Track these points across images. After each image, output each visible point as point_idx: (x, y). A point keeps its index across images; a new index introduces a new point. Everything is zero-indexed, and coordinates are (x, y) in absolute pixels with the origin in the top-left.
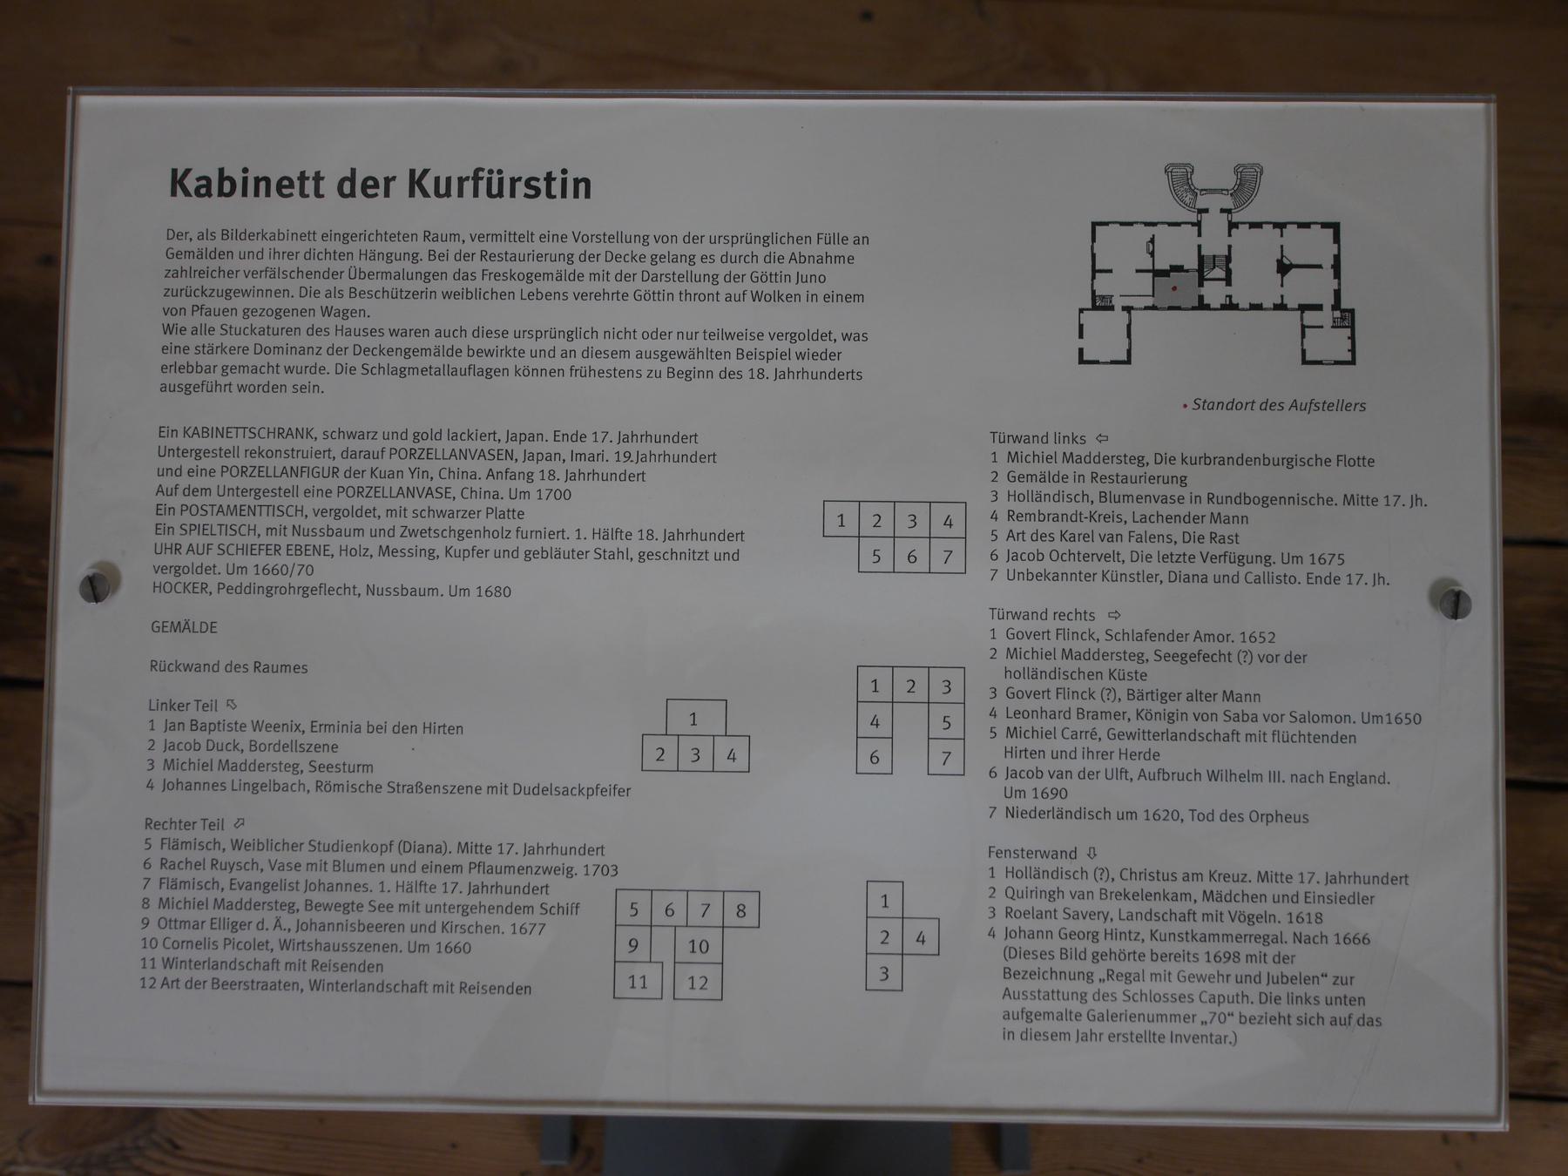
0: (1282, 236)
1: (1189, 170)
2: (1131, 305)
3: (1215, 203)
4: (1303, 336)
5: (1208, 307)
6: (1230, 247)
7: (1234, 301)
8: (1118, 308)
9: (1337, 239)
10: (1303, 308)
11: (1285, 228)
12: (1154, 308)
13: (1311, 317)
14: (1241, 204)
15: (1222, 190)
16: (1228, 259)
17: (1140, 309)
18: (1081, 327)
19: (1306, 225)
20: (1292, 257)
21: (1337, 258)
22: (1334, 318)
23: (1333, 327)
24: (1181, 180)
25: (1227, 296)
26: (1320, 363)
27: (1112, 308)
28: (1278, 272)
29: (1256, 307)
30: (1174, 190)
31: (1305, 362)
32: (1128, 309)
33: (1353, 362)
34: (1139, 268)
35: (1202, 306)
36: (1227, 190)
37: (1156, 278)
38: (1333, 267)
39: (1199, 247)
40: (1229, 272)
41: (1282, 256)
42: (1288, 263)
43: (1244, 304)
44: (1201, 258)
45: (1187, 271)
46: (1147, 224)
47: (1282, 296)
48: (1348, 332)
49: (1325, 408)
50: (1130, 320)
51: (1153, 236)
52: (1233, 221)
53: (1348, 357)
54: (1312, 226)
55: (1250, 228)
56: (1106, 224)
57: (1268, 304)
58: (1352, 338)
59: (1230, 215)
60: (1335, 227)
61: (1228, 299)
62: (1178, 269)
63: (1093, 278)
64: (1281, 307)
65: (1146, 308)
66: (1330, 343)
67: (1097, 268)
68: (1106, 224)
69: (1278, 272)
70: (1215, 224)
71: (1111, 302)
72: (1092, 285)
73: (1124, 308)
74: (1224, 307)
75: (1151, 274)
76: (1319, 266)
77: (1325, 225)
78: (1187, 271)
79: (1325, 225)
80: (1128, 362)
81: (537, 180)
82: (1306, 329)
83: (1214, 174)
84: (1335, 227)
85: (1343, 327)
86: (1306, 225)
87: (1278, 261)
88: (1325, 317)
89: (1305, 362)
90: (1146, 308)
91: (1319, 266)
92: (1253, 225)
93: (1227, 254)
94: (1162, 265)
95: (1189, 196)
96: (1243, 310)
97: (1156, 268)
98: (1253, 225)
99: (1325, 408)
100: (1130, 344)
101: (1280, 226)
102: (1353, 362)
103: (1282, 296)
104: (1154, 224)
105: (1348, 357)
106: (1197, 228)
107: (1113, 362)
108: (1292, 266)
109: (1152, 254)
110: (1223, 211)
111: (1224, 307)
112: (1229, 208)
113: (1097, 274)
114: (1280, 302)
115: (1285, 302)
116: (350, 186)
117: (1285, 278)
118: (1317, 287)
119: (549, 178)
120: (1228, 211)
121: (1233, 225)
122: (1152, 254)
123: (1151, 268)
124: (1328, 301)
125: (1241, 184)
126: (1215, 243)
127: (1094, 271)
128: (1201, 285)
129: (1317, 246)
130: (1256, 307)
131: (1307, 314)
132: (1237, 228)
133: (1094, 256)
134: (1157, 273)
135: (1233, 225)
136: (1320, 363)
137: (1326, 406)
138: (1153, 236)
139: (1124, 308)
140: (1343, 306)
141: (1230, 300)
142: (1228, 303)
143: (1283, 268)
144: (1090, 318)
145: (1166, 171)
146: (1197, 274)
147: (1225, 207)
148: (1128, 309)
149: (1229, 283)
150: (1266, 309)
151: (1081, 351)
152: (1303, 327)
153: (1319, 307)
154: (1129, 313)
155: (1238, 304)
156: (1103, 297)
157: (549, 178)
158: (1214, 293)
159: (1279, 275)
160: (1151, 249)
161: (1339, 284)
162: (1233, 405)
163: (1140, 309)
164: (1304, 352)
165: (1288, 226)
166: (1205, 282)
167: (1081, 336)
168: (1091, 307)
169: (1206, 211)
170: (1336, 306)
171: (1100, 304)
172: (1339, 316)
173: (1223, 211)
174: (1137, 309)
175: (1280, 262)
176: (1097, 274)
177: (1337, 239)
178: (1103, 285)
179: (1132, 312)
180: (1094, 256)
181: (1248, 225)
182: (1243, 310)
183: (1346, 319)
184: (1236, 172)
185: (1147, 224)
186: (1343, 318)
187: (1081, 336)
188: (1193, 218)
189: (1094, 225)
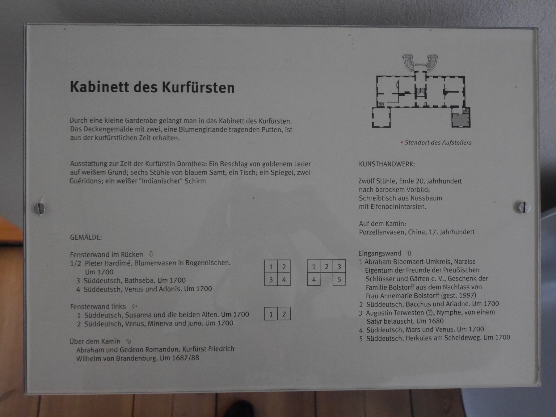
0: (445, 81)
3: (421, 69)
5: (418, 107)
6: (426, 85)
7: (428, 105)
8: (386, 107)
9: (464, 82)
10: (452, 107)
11: (446, 78)
12: (399, 107)
13: (455, 111)
14: (430, 70)
15: (423, 64)
16: (426, 89)
18: (373, 114)
19: (453, 77)
21: (464, 89)
22: (463, 111)
24: (409, 60)
25: (425, 103)
27: (383, 107)
28: (443, 94)
29: (435, 107)
30: (406, 64)
32: (389, 108)
34: (393, 93)
35: (416, 106)
36: (425, 64)
37: (400, 96)
38: (463, 92)
39: (415, 85)
40: (426, 94)
41: (445, 88)
42: (447, 91)
43: (431, 106)
44: (416, 89)
45: (411, 94)
46: (396, 77)
47: (445, 103)
51: (399, 81)
52: (427, 75)
54: (455, 77)
55: (433, 78)
56: (382, 76)
57: (440, 106)
58: (469, 118)
59: (426, 73)
60: (463, 78)
61: (425, 104)
62: (408, 93)
63: (377, 96)
64: (444, 107)
65: (396, 107)
67: (378, 93)
68: (382, 76)
69: (443, 94)
70: (421, 76)
71: (383, 105)
72: (377, 99)
73: (388, 107)
74: (424, 107)
75: (398, 95)
76: (458, 92)
77: (460, 77)
78: (411, 94)
79: (460, 77)
80: (390, 127)
82: (453, 115)
83: (421, 58)
84: (463, 78)
85: (466, 114)
86: (453, 77)
87: (443, 90)
88: (460, 111)
90: (396, 107)
91: (458, 92)
92: (435, 77)
93: (425, 87)
94: (402, 91)
95: (412, 66)
96: (431, 108)
97: (400, 92)
98: (435, 77)
101: (444, 77)
103: (445, 103)
104: (399, 77)
106: (414, 78)
107: (384, 127)
108: (448, 92)
109: (398, 87)
110: (423, 72)
111: (424, 107)
112: (426, 71)
113: (378, 95)
114: (444, 105)
115: (446, 105)
117: (446, 96)
118: (457, 99)
120: (426, 72)
121: (427, 77)
122: (398, 87)
123: (398, 93)
124: (461, 105)
125: (430, 62)
126: (421, 84)
127: (377, 94)
128: (416, 98)
129: (457, 84)
130: (435, 107)
131: (454, 109)
132: (429, 78)
134: (400, 94)
135: (427, 77)
138: (399, 81)
139: (388, 107)
140: (466, 106)
141: (426, 105)
142: (425, 105)
143: (445, 93)
144: (376, 111)
145: (403, 57)
146: (414, 95)
147: (424, 71)
148: (389, 108)
149: (426, 98)
150: (439, 107)
151: (373, 123)
152: (452, 114)
153: (458, 107)
154: (390, 109)
155: (429, 106)
156: (380, 103)
158: (421, 102)
159: (444, 95)
160: (398, 86)
161: (465, 98)
165: (447, 77)
166: (417, 98)
167: (373, 117)
168: (376, 107)
169: (417, 72)
170: (464, 106)
171: (380, 106)
172: (465, 110)
173: (423, 72)
174: (392, 108)
175: (444, 90)
176: (378, 95)
177: (464, 82)
178: (381, 99)
179: (391, 108)
181: (432, 77)
182: (431, 108)
184: (428, 58)
185: (396, 77)
186: (466, 111)
187: (373, 117)
188: (413, 74)
189: (377, 77)
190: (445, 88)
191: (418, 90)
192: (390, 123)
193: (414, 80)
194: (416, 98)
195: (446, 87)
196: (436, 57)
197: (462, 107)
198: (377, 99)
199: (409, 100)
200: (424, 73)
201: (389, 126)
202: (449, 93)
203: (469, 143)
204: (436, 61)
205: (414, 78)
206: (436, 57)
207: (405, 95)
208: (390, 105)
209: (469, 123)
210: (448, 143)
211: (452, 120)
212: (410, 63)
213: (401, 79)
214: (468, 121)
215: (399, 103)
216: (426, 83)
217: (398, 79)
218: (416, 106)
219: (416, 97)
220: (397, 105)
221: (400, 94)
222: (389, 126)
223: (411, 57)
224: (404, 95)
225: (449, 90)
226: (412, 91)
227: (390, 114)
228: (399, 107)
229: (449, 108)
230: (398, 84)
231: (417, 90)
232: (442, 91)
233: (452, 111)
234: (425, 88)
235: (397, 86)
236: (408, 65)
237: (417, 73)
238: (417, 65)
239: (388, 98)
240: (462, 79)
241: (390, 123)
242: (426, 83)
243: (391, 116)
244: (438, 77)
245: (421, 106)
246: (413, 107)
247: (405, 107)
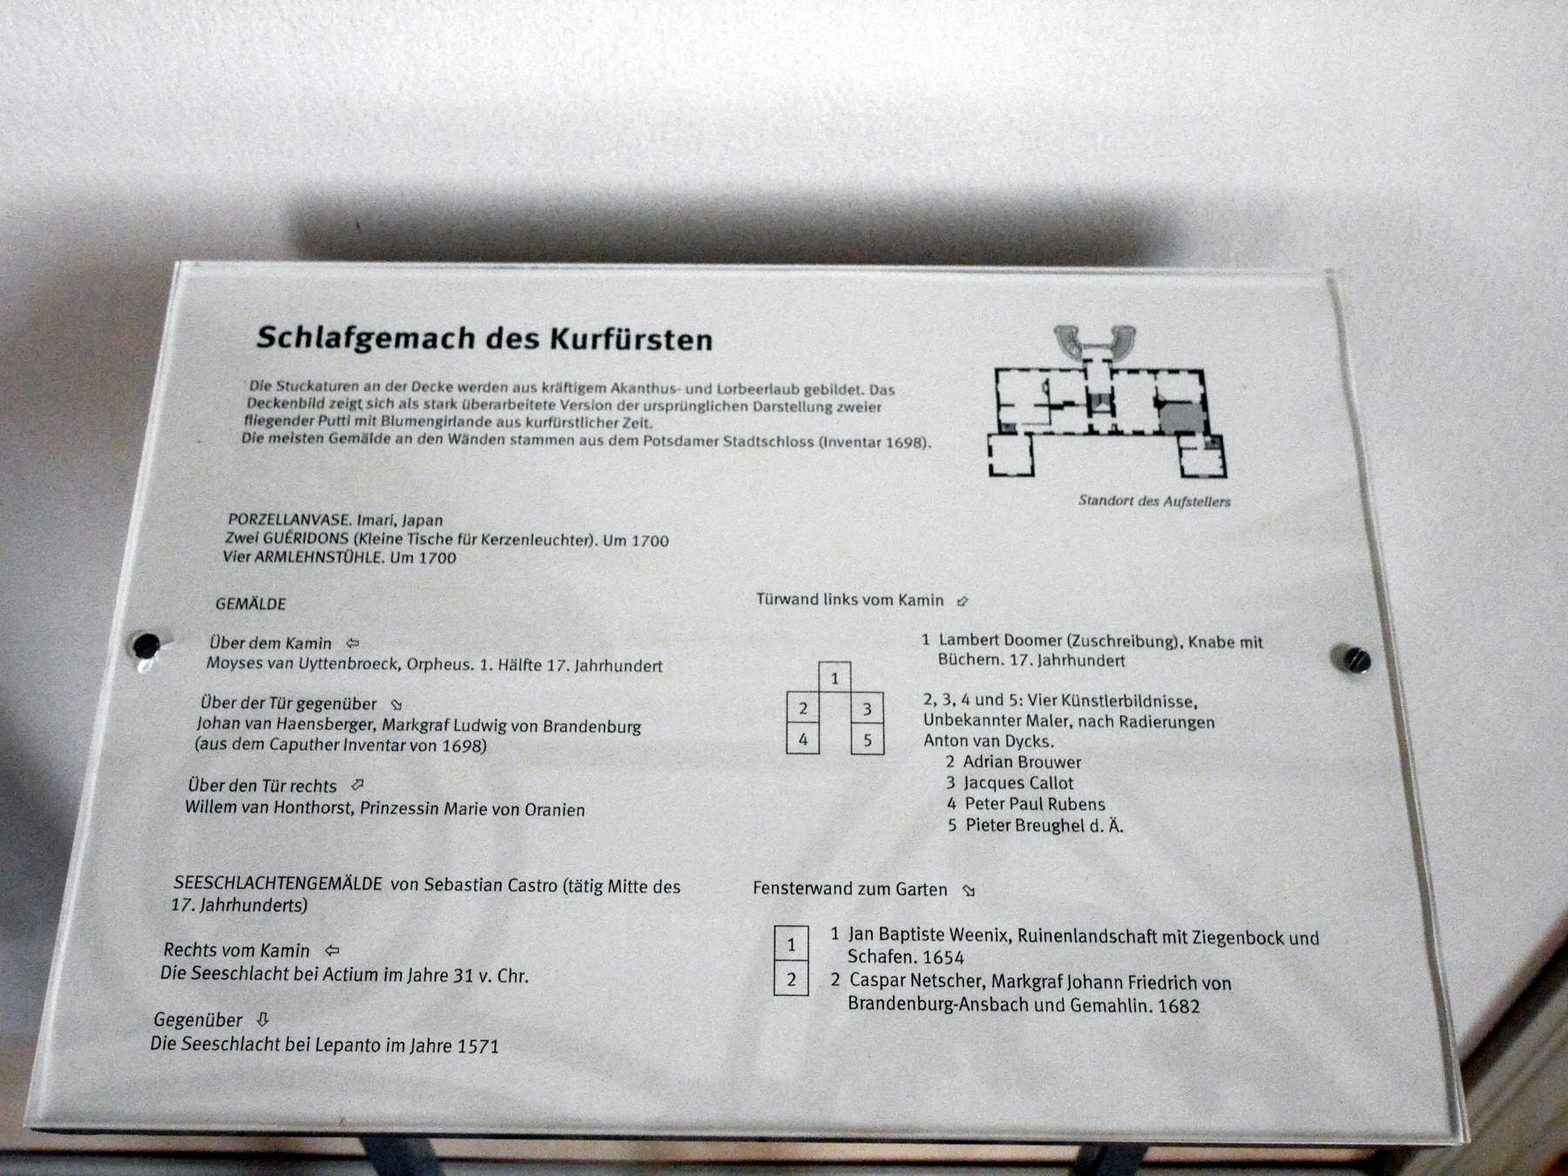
5: (1097, 433)
9: (1202, 382)
12: (1052, 433)
16: (1112, 397)
18: (990, 449)
20: (1166, 395)
21: (1204, 397)
27: (1015, 433)
32: (1030, 434)
35: (1092, 431)
37: (1053, 412)
44: (1089, 397)
45: (1078, 405)
62: (1071, 404)
63: (999, 409)
65: (1046, 434)
67: (1002, 402)
72: (998, 416)
74: (1111, 433)
77: (1191, 372)
79: (1191, 372)
84: (1201, 373)
90: (1046, 434)
93: (1110, 392)
94: (1056, 400)
108: (1166, 402)
109: (1048, 393)
111: (1111, 433)
116: (496, 340)
122: (1048, 393)
126: (1100, 383)
127: (999, 406)
134: (1052, 407)
141: (1116, 429)
144: (997, 442)
146: (1084, 410)
148: (1030, 434)
149: (1113, 413)
151: (991, 467)
156: (1007, 425)
158: (1103, 422)
159: (1156, 410)
167: (990, 454)
171: (1006, 430)
177: (1202, 382)
178: (1007, 416)
179: (1034, 437)
187: (990, 454)
190: (1157, 395)
199: (1076, 419)
207: (1066, 408)
208: (1030, 429)
216: (1112, 383)
218: (1092, 431)
219: (1090, 413)
220: (1047, 429)
221: (1052, 407)
226: (1081, 399)
228: (1052, 433)
231: (1093, 398)
232: (1152, 402)
239: (1023, 414)
242: (1112, 383)
246: (1085, 434)
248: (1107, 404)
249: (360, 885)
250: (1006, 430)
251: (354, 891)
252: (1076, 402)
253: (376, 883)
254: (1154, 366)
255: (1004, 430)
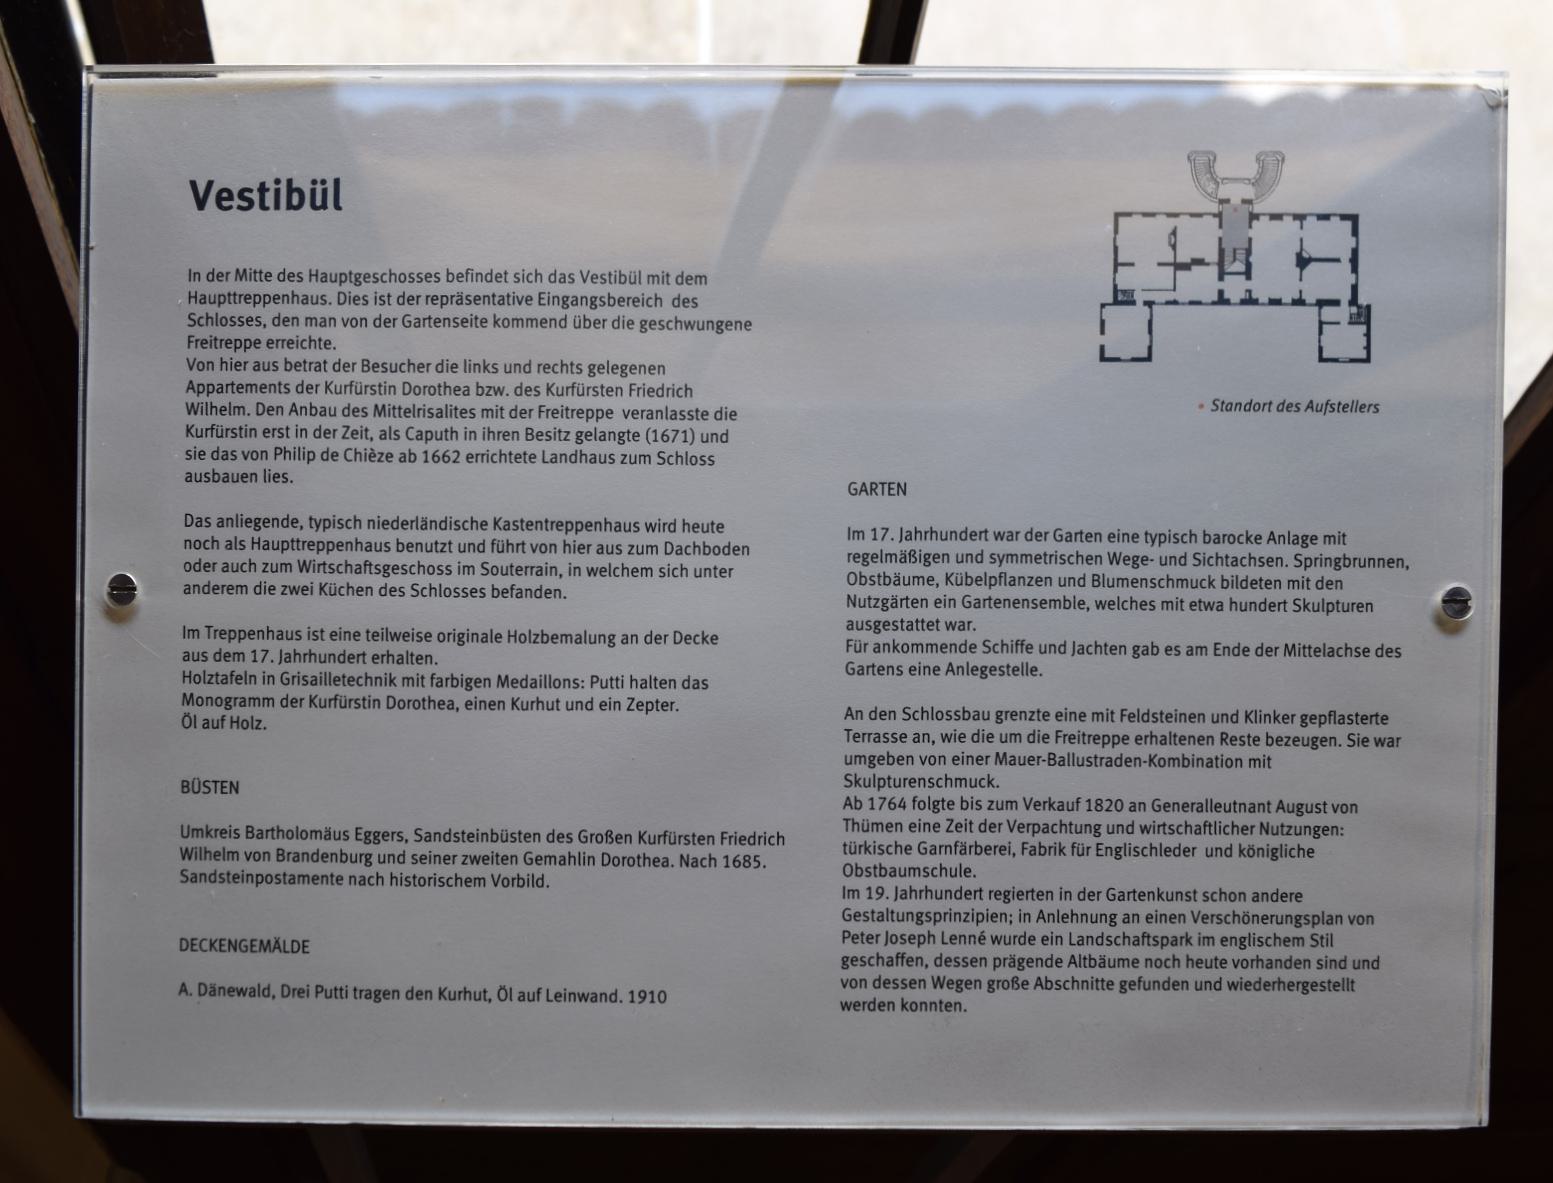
0: (1302, 228)
1: (1212, 158)
2: (1152, 299)
4: (1321, 332)
5: (1227, 302)
7: (1254, 296)
8: (1140, 303)
9: (1355, 232)
10: (1321, 303)
12: (1175, 302)
13: (1329, 313)
14: (1260, 196)
16: (1249, 252)
17: (1162, 304)
18: (1103, 323)
20: (1311, 250)
21: (1355, 252)
22: (1351, 315)
23: (1350, 323)
26: (1335, 360)
27: (1133, 303)
31: (1322, 359)
32: (1149, 304)
33: (1367, 360)
35: (1222, 300)
36: (1249, 180)
37: (1179, 273)
40: (1249, 266)
41: (1302, 249)
43: (1264, 299)
44: (1221, 252)
45: (1208, 264)
46: (1170, 215)
47: (1301, 292)
48: (1363, 329)
49: (1341, 409)
50: (1151, 315)
51: (1176, 228)
53: (1363, 355)
57: (1287, 299)
58: (1368, 335)
60: (1354, 219)
62: (1199, 262)
63: (1115, 271)
64: (1299, 302)
65: (1168, 303)
66: (1346, 339)
67: (1120, 260)
69: (1297, 265)
71: (1132, 296)
72: (1114, 279)
74: (1244, 302)
75: (1172, 268)
76: (1337, 260)
77: (1344, 217)
79: (1344, 217)
80: (1149, 359)
81: (250, 191)
82: (1324, 326)
84: (1354, 219)
88: (1343, 312)
89: (1322, 359)
90: (1168, 303)
91: (1337, 260)
93: (1246, 246)
94: (1183, 258)
96: (1263, 304)
97: (1179, 260)
98: (1276, 217)
99: (1341, 409)
100: (1151, 341)
101: (1300, 217)
102: (1367, 360)
103: (1301, 292)
104: (1176, 215)
105: (1363, 355)
106: (1217, 220)
108: (1310, 260)
109: (1174, 247)
111: (1244, 302)
113: (1120, 268)
114: (1297, 296)
115: (1303, 297)
117: (1304, 272)
118: (1331, 281)
119: (263, 189)
122: (1174, 247)
123: (1172, 260)
127: (1117, 265)
129: (1332, 239)
133: (1116, 249)
134: (1179, 267)
135: (1254, 217)
136: (1335, 360)
137: (1341, 407)
138: (1176, 228)
141: (1250, 295)
143: (1303, 262)
144: (1111, 313)
145: (1189, 157)
146: (1214, 270)
148: (1149, 304)
149: (1248, 274)
151: (1102, 348)
152: (1321, 323)
153: (1336, 303)
154: (1150, 307)
156: (1124, 292)
157: (263, 189)
158: (1235, 288)
159: (1298, 270)
160: (1173, 242)
162: (1251, 406)
163: (1162, 304)
164: (1321, 349)
166: (1226, 277)
167: (1102, 332)
170: (1353, 301)
171: (1122, 298)
174: (1158, 304)
175: (1299, 256)
176: (1120, 268)
177: (1355, 232)
179: (1154, 307)
180: (1116, 249)
183: (1363, 316)
184: (1258, 160)
185: (1170, 215)
186: (1359, 314)
187: (1102, 332)
188: (1214, 208)
190: (1302, 249)
191: (1228, 258)
192: (1150, 348)
193: (1217, 224)
194: (1221, 278)
195: (1304, 247)
196: (1280, 158)
197: (1347, 303)
198: (1114, 279)
199: (1202, 282)
200: (1247, 206)
201: (1145, 355)
202: (1313, 266)
203: (1372, 408)
204: (1278, 172)
205: (1217, 220)
206: (1280, 158)
207: (1194, 268)
208: (1150, 297)
209: (1365, 352)
210: (1319, 409)
211: (1319, 341)
212: (1208, 176)
213: (1183, 223)
214: (1365, 344)
215: (1174, 290)
217: (1173, 222)
218: (1222, 300)
220: (1171, 296)
221: (1179, 267)
222: (1145, 355)
223: (1212, 158)
224: (1189, 269)
225: (1314, 256)
226: (1212, 256)
227: (1150, 323)
228: (1175, 302)
229: (1311, 305)
230: (1172, 237)
231: (1226, 253)
233: (1320, 315)
234: (1246, 250)
235: (1170, 239)
236: (1202, 182)
237: (1225, 205)
238: (1225, 181)
240: (1348, 224)
241: (1150, 348)
243: (1154, 328)
244: (1285, 218)
245: (1235, 299)
246: (1214, 303)
247: (1192, 303)
248: (1241, 262)
249: (288, 948)
250: (1122, 298)
251: (283, 954)
252: (1206, 261)
253: (304, 946)
254: (1300, 211)
255: (1120, 297)
